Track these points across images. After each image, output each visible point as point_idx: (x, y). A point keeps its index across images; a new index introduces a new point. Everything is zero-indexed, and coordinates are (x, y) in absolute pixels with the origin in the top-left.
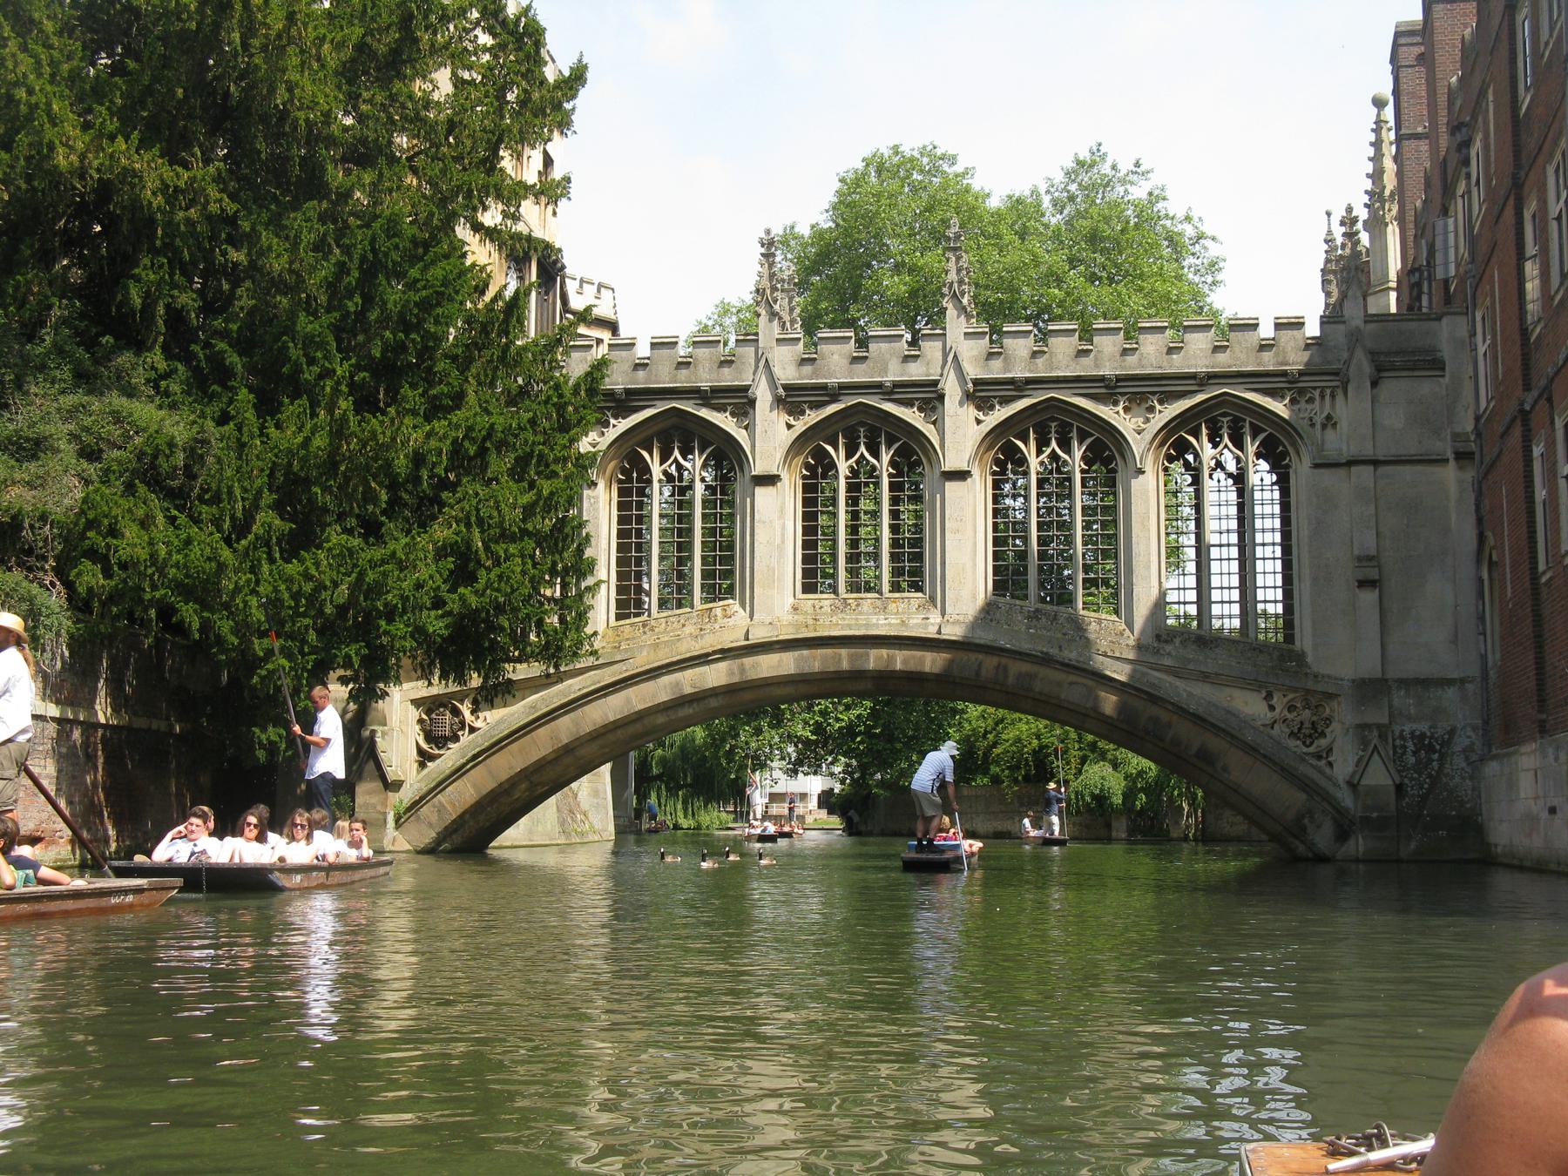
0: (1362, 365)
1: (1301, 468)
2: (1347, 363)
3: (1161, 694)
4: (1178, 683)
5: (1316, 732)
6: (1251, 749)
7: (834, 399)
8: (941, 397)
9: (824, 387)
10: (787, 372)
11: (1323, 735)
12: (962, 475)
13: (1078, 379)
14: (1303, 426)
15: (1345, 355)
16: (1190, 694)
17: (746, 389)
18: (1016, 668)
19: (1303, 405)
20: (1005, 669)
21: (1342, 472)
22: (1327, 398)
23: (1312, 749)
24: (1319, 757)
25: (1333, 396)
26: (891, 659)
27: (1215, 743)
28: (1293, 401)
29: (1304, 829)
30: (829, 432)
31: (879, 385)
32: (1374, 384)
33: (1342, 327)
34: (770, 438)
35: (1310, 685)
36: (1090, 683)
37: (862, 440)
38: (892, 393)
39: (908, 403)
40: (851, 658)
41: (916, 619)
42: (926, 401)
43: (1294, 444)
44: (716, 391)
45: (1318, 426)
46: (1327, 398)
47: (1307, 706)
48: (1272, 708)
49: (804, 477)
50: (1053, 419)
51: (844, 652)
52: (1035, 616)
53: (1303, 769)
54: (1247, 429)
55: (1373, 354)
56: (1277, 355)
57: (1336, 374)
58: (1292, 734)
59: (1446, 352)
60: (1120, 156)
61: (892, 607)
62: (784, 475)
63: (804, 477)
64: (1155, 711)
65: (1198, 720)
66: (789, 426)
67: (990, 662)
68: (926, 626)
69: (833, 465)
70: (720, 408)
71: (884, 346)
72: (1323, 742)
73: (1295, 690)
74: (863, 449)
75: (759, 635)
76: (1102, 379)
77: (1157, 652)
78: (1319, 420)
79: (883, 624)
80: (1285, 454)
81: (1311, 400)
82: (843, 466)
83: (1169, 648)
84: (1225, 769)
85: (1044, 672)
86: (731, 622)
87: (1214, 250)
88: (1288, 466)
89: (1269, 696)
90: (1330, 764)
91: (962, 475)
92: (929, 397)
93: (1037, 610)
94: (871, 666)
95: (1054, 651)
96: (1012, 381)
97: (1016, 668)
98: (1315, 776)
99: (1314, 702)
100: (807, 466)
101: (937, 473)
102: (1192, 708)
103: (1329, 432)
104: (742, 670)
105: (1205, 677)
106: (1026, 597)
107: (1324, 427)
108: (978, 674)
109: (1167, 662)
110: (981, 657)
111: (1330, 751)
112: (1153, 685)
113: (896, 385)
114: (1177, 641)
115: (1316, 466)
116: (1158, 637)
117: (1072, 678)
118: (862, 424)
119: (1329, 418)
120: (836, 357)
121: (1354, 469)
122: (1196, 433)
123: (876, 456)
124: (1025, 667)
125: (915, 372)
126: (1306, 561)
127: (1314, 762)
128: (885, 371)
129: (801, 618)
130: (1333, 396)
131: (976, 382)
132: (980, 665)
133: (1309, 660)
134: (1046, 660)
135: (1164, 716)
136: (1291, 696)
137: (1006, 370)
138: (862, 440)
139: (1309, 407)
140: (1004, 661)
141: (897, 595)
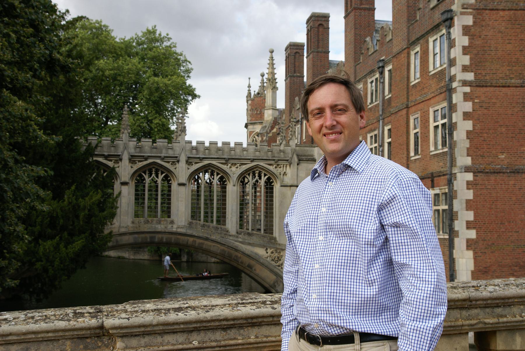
0: (296, 159)
1: (277, 187)
2: (292, 158)
3: (238, 249)
4: (243, 246)
5: (279, 259)
6: (262, 264)
7: (146, 159)
8: (178, 161)
9: (143, 156)
10: (132, 151)
11: (280, 260)
12: (183, 185)
13: (218, 158)
14: (278, 174)
15: (290, 156)
16: (246, 249)
17: (119, 155)
18: (198, 241)
19: (278, 169)
20: (195, 241)
21: (288, 188)
22: (285, 167)
23: (277, 264)
24: (279, 266)
25: (286, 167)
26: (162, 238)
27: (252, 262)
28: (276, 167)
29: (275, 286)
30: (144, 170)
31: (160, 157)
32: (298, 164)
33: (289, 148)
34: (125, 170)
35: (278, 247)
36: (219, 246)
37: (154, 172)
38: (163, 159)
39: (168, 162)
40: (151, 238)
41: (170, 226)
42: (174, 162)
43: (275, 179)
44: (109, 156)
45: (282, 175)
46: (285, 167)
47: (277, 252)
48: (267, 253)
49: (136, 183)
50: (210, 169)
51: (148, 236)
52: (203, 226)
53: (275, 270)
54: (263, 175)
55: (298, 155)
56: (272, 154)
57: (287, 160)
58: (273, 260)
59: (316, 156)
60: (162, 31)
61: (162, 222)
62: (130, 182)
63: (136, 183)
64: (237, 253)
65: (248, 256)
66: (132, 167)
67: (191, 239)
68: (172, 229)
69: (144, 179)
70: (111, 161)
71: (160, 143)
72: (281, 262)
73: (274, 248)
74: (153, 175)
75: (123, 230)
76: (224, 159)
77: (237, 237)
78: (282, 173)
79: (160, 227)
80: (272, 182)
81: (280, 167)
82: (148, 180)
83: (240, 236)
84: (255, 270)
85: (206, 242)
86: (113, 226)
87: (190, 66)
88: (273, 185)
89: (267, 249)
90: (282, 268)
91: (183, 185)
92: (176, 160)
93: (204, 224)
94: (156, 240)
95: (209, 236)
96: (199, 158)
97: (198, 241)
98: (278, 271)
99: (278, 251)
100: (136, 179)
101: (176, 183)
102: (247, 252)
103: (285, 176)
104: (117, 241)
105: (249, 244)
106: (200, 220)
107: (283, 175)
108: (187, 243)
109: (240, 240)
110: (188, 238)
111: (282, 264)
112: (236, 246)
113: (165, 157)
114: (242, 234)
115: (281, 186)
116: (237, 233)
117: (214, 244)
118: (154, 168)
119: (285, 173)
120: (147, 147)
121: (292, 188)
122: (249, 175)
123: (157, 177)
124: (201, 241)
125: (171, 153)
126: (277, 212)
127: (278, 267)
128: (161, 153)
129: (134, 225)
130: (286, 167)
131: (189, 158)
132: (188, 240)
133: (278, 239)
134: (207, 239)
135: (239, 255)
136: (272, 250)
137: (197, 154)
138: (154, 172)
139: (280, 169)
140: (195, 239)
141: (163, 219)
